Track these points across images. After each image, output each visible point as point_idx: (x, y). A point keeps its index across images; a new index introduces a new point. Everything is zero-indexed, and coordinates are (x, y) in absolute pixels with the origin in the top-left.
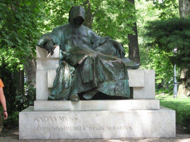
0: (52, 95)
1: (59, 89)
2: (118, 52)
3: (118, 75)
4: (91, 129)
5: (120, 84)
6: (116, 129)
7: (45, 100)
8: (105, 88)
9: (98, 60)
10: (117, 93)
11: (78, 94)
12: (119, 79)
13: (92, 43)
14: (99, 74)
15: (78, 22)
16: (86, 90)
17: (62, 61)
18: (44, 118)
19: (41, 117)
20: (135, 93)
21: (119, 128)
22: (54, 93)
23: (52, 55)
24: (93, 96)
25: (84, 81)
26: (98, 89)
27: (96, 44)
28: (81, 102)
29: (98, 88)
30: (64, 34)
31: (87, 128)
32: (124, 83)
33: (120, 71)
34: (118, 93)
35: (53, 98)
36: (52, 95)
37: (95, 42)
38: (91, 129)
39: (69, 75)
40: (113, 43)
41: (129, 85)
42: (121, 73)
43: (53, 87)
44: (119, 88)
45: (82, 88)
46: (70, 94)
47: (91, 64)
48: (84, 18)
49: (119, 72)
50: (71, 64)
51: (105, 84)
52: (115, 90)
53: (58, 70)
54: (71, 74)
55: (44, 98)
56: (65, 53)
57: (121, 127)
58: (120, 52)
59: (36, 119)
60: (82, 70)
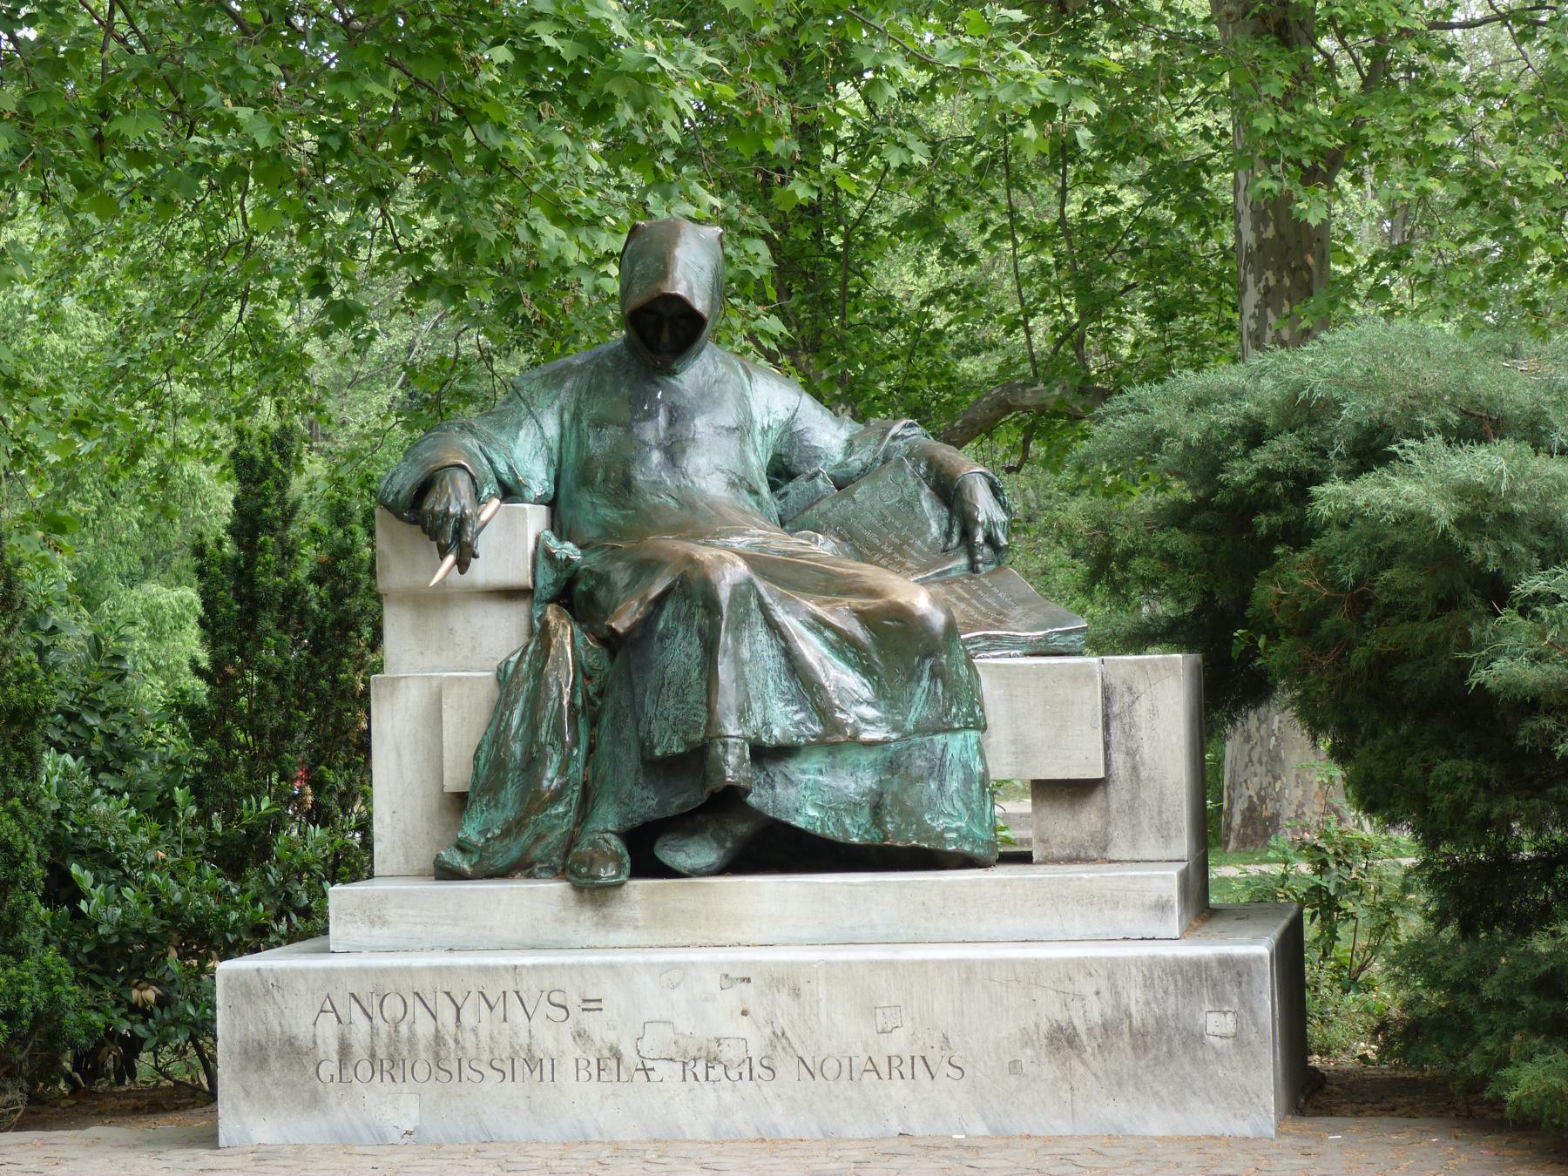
0: (462, 847)
2: (956, 539)
7: (420, 875)
8: (807, 797)
12: (910, 726)
15: (666, 337)
21: (884, 1069)
22: (471, 831)
23: (462, 572)
24: (728, 844)
25: (653, 747)
30: (576, 417)
31: (662, 1069)
33: (913, 676)
34: (898, 827)
36: (462, 847)
40: (929, 467)
42: (925, 683)
43: (474, 786)
45: (645, 794)
46: (571, 841)
47: (700, 630)
48: (700, 305)
54: (588, 700)
56: (568, 550)
57: (895, 1062)
58: (967, 535)
59: (328, 1006)
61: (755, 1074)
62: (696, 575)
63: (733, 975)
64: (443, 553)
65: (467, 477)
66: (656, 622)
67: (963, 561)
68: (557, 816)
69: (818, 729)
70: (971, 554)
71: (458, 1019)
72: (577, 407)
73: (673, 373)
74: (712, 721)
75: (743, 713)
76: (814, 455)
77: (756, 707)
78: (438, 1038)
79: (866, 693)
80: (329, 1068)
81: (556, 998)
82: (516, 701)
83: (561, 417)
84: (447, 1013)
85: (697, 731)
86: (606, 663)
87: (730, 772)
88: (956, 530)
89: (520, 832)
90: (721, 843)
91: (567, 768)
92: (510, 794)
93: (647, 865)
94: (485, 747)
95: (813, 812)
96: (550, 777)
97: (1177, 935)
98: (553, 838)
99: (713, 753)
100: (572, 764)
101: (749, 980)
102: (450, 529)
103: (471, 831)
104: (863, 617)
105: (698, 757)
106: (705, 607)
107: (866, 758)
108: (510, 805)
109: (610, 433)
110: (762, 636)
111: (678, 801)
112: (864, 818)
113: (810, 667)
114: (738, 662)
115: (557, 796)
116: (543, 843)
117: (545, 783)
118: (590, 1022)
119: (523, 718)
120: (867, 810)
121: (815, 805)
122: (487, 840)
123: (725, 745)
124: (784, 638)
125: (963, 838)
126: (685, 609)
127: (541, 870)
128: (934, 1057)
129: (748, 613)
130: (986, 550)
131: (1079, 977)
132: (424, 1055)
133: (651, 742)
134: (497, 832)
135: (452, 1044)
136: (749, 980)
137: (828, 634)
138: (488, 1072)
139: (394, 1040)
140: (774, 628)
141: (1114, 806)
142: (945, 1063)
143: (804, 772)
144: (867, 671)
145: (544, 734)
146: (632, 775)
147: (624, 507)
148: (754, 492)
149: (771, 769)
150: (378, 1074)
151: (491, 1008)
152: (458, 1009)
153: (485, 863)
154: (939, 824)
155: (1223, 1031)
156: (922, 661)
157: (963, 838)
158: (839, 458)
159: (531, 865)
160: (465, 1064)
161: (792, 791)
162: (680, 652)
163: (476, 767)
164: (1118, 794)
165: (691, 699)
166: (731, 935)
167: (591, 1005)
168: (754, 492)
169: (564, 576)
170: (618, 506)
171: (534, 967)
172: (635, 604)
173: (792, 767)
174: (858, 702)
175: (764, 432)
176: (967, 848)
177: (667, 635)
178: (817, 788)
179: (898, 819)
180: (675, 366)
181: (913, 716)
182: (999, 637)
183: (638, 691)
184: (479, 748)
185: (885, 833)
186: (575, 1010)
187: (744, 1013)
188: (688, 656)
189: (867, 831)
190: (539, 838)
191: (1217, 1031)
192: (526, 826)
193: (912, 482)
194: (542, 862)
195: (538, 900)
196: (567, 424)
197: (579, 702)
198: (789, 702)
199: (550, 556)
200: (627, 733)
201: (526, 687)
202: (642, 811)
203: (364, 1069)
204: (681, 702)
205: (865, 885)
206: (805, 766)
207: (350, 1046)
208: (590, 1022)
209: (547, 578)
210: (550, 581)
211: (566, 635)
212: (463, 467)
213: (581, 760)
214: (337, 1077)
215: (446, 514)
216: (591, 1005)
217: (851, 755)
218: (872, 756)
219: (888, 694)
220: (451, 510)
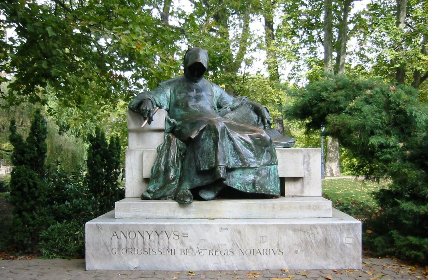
0: (149, 192)
1: (160, 182)
4: (211, 254)
5: (264, 173)
6: (255, 254)
8: (238, 180)
9: (226, 132)
10: (257, 189)
11: (191, 190)
12: (262, 164)
14: (227, 156)
15: (196, 73)
16: (204, 184)
17: (168, 134)
19: (124, 232)
20: (289, 188)
21: (262, 252)
22: (151, 188)
23: (149, 124)
25: (200, 168)
26: (224, 182)
28: (195, 203)
29: (225, 180)
30: (174, 91)
32: (269, 172)
33: (263, 151)
34: (259, 189)
35: (148, 195)
36: (149, 192)
37: (225, 105)
38: (211, 254)
39: (177, 157)
40: (252, 106)
41: (278, 176)
42: (265, 153)
43: (151, 177)
44: (261, 180)
46: (177, 191)
47: (213, 139)
48: (205, 65)
49: (262, 152)
51: (237, 174)
52: (254, 184)
53: (160, 149)
54: (181, 156)
55: (135, 196)
56: (173, 121)
57: (265, 251)
58: (263, 121)
59: (115, 234)
61: (228, 254)
63: (223, 228)
64: (145, 119)
66: (201, 136)
67: (262, 127)
68: (173, 185)
69: (241, 164)
71: (150, 238)
72: (174, 89)
73: (197, 82)
75: (224, 159)
76: (225, 103)
77: (227, 158)
79: (252, 155)
83: (171, 91)
84: (147, 237)
85: (213, 164)
86: (185, 147)
87: (221, 175)
88: (260, 120)
89: (164, 189)
90: (215, 192)
91: (176, 173)
92: (161, 178)
93: (197, 197)
94: (155, 167)
95: (239, 185)
96: (172, 175)
97: (331, 216)
98: (172, 190)
100: (177, 172)
101: (227, 229)
102: (147, 114)
104: (251, 137)
105: (213, 170)
107: (252, 171)
108: (161, 182)
109: (183, 95)
110: (228, 140)
111: (206, 182)
112: (251, 187)
113: (239, 148)
114: (223, 147)
115: (174, 180)
117: (170, 177)
119: (164, 160)
120: (251, 184)
121: (239, 183)
122: (155, 190)
123: (220, 168)
124: (233, 141)
125: (274, 191)
126: (209, 133)
127: (169, 198)
128: (275, 249)
131: (314, 229)
133: (200, 167)
134: (158, 188)
135: (147, 244)
136: (227, 229)
137: (242, 141)
140: (230, 138)
141: (305, 183)
143: (237, 175)
144: (252, 150)
145: (170, 165)
147: (187, 111)
148: (215, 109)
149: (229, 174)
151: (158, 236)
153: (155, 196)
154: (269, 188)
155: (350, 242)
156: (265, 148)
157: (274, 191)
158: (231, 104)
159: (166, 196)
160: (151, 250)
161: (234, 179)
162: (208, 144)
163: (152, 172)
164: (306, 181)
165: (211, 156)
166: (218, 216)
168: (215, 109)
169: (172, 127)
170: (185, 111)
171: (170, 225)
172: (196, 132)
173: (234, 173)
174: (250, 158)
176: (275, 194)
177: (204, 139)
178: (240, 179)
179: (259, 187)
180: (197, 81)
181: (262, 162)
182: (278, 143)
183: (196, 154)
184: (153, 167)
185: (256, 190)
186: (180, 236)
188: (210, 145)
190: (168, 190)
191: (348, 243)
192: (166, 187)
194: (169, 196)
196: (172, 93)
197: (179, 156)
198: (234, 157)
199: (169, 122)
200: (193, 164)
201: (165, 153)
202: (196, 184)
203: (124, 251)
209: (168, 127)
212: (149, 99)
215: (146, 110)
217: (248, 170)
219: (258, 156)
220: (147, 109)
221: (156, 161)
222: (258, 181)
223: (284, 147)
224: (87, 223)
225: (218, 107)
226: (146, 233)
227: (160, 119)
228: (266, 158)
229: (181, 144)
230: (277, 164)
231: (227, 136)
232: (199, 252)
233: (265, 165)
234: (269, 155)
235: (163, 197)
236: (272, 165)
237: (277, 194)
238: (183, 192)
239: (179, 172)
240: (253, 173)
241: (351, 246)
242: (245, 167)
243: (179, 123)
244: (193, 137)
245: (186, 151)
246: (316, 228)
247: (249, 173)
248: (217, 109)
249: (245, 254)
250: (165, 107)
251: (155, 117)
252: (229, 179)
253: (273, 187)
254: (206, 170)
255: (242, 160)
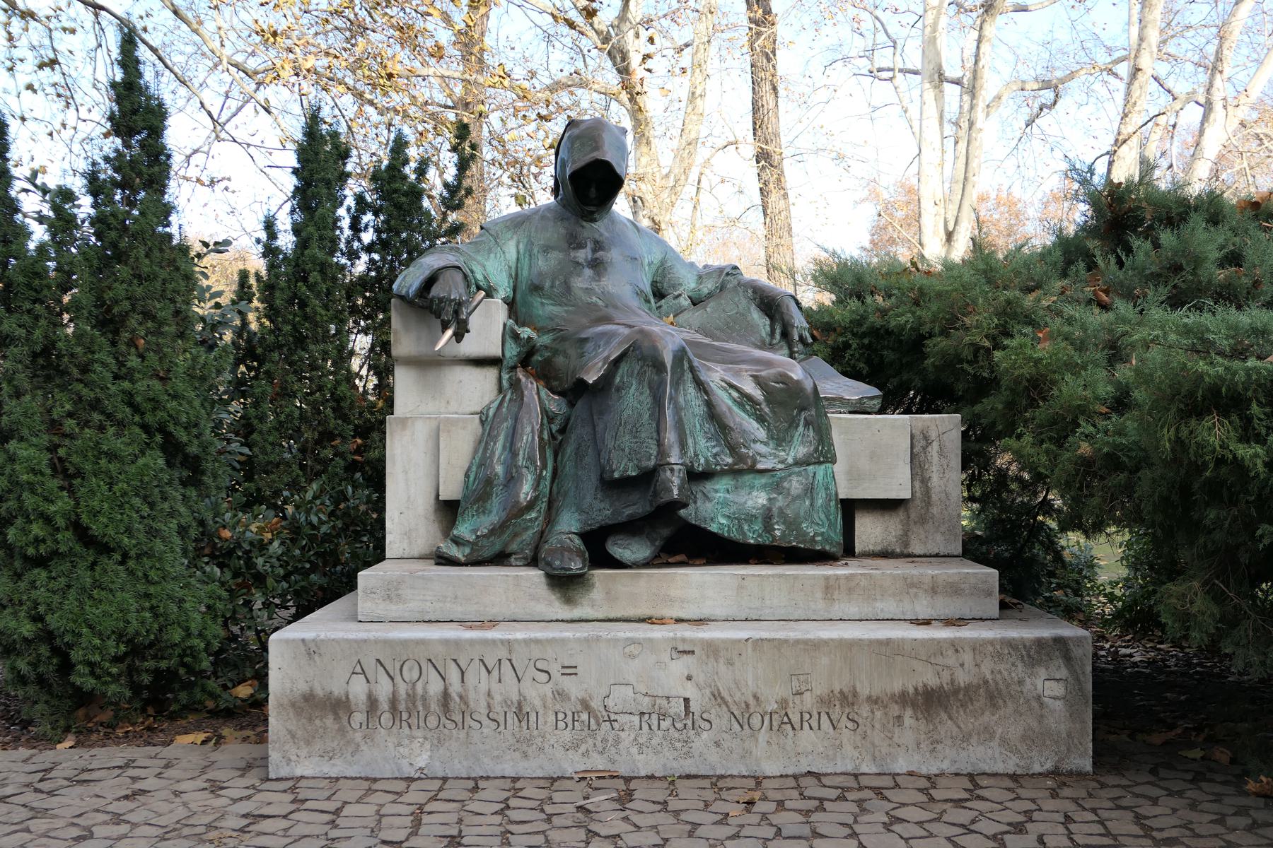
0: (457, 542)
2: (778, 336)
3: (780, 439)
5: (795, 485)
7: (422, 558)
8: (719, 508)
9: (686, 365)
10: (778, 533)
11: (583, 536)
12: (790, 460)
13: (659, 294)
15: (593, 193)
16: (622, 519)
18: (398, 666)
20: (869, 531)
23: (458, 341)
24: (657, 543)
26: (682, 512)
27: (677, 297)
28: (600, 574)
29: (685, 506)
33: (793, 424)
35: (455, 552)
39: (541, 439)
41: (837, 494)
42: (801, 429)
43: (465, 496)
45: (602, 505)
46: (542, 536)
50: (555, 383)
51: (720, 489)
52: (767, 517)
54: (552, 436)
56: (526, 332)
57: (806, 716)
58: (785, 335)
59: (358, 669)
60: (601, 413)
62: (646, 344)
64: (445, 327)
65: (461, 275)
66: (614, 377)
69: (730, 460)
70: (790, 347)
72: (529, 240)
73: (594, 220)
74: (662, 452)
77: (690, 441)
78: (446, 695)
79: (761, 433)
80: (359, 718)
81: (539, 665)
82: (498, 435)
84: (453, 675)
87: (676, 492)
88: (778, 331)
89: (503, 532)
90: (652, 541)
91: (538, 485)
93: (603, 560)
94: (474, 469)
95: (724, 521)
96: (526, 490)
98: (528, 536)
99: (662, 476)
101: (693, 652)
102: (451, 309)
103: (464, 529)
104: (757, 380)
105: (648, 478)
106: (654, 366)
110: (691, 390)
111: (628, 511)
112: (758, 527)
114: (678, 410)
115: (531, 506)
116: (519, 539)
117: (522, 496)
118: (568, 684)
119: (504, 447)
122: (478, 537)
123: (672, 470)
124: (706, 392)
129: (683, 370)
130: (800, 346)
132: (434, 707)
133: (611, 466)
135: (457, 699)
138: (486, 721)
139: (411, 697)
140: (700, 385)
141: (913, 515)
142: (844, 717)
143: (716, 491)
144: (761, 419)
145: (521, 461)
146: (592, 492)
148: (648, 301)
150: (397, 722)
151: (489, 672)
152: (463, 673)
158: (693, 285)
159: (509, 555)
160: (467, 718)
161: (709, 505)
162: (633, 399)
163: (466, 483)
165: (643, 435)
167: (570, 670)
168: (648, 301)
169: (525, 350)
173: (709, 486)
174: (755, 441)
175: (650, 264)
176: (827, 548)
178: (725, 503)
180: (597, 216)
183: (600, 428)
184: (469, 469)
187: (689, 678)
189: (760, 536)
190: (516, 535)
191: (1052, 694)
192: (508, 527)
193: (744, 302)
195: (520, 586)
197: (546, 436)
198: (709, 439)
199: (516, 337)
200: (589, 459)
201: (507, 425)
203: (386, 718)
204: (635, 437)
205: (773, 576)
206: (717, 487)
207: (376, 701)
208: (568, 684)
209: (512, 351)
210: (515, 353)
211: (532, 388)
212: (458, 268)
213: (549, 479)
214: (364, 727)
216: (570, 670)
217: (748, 478)
218: (763, 481)
221: (475, 452)
222: (780, 509)
223: (850, 413)
224: (273, 637)
225: (654, 295)
226: (453, 665)
227: (488, 328)
228: (802, 442)
229: (555, 404)
230: (834, 462)
231: (690, 375)
232: (610, 721)
233: (797, 463)
234: (811, 433)
235: (501, 559)
236: (820, 463)
237: (833, 550)
238: (560, 541)
239: (548, 483)
240: (764, 487)
241: (1058, 703)
242: (743, 469)
243: (546, 339)
244: (591, 379)
245: (568, 420)
246: (957, 651)
247: (752, 487)
248: (652, 301)
249: (746, 727)
250: (502, 294)
251: (474, 322)
252: (695, 502)
253: (820, 527)
254: (629, 478)
255: (733, 449)
